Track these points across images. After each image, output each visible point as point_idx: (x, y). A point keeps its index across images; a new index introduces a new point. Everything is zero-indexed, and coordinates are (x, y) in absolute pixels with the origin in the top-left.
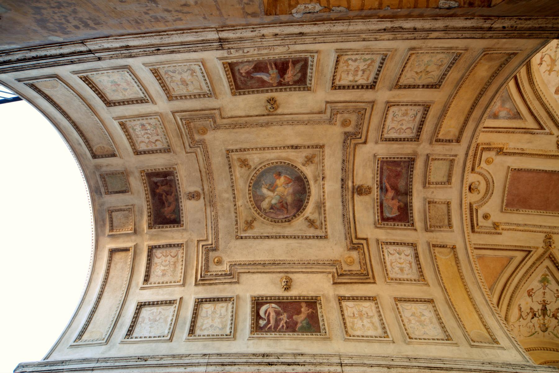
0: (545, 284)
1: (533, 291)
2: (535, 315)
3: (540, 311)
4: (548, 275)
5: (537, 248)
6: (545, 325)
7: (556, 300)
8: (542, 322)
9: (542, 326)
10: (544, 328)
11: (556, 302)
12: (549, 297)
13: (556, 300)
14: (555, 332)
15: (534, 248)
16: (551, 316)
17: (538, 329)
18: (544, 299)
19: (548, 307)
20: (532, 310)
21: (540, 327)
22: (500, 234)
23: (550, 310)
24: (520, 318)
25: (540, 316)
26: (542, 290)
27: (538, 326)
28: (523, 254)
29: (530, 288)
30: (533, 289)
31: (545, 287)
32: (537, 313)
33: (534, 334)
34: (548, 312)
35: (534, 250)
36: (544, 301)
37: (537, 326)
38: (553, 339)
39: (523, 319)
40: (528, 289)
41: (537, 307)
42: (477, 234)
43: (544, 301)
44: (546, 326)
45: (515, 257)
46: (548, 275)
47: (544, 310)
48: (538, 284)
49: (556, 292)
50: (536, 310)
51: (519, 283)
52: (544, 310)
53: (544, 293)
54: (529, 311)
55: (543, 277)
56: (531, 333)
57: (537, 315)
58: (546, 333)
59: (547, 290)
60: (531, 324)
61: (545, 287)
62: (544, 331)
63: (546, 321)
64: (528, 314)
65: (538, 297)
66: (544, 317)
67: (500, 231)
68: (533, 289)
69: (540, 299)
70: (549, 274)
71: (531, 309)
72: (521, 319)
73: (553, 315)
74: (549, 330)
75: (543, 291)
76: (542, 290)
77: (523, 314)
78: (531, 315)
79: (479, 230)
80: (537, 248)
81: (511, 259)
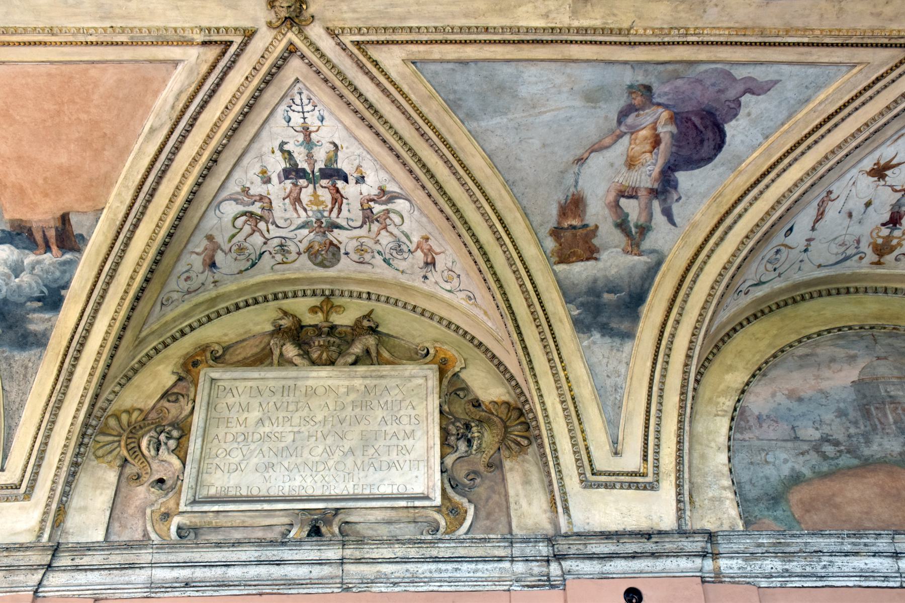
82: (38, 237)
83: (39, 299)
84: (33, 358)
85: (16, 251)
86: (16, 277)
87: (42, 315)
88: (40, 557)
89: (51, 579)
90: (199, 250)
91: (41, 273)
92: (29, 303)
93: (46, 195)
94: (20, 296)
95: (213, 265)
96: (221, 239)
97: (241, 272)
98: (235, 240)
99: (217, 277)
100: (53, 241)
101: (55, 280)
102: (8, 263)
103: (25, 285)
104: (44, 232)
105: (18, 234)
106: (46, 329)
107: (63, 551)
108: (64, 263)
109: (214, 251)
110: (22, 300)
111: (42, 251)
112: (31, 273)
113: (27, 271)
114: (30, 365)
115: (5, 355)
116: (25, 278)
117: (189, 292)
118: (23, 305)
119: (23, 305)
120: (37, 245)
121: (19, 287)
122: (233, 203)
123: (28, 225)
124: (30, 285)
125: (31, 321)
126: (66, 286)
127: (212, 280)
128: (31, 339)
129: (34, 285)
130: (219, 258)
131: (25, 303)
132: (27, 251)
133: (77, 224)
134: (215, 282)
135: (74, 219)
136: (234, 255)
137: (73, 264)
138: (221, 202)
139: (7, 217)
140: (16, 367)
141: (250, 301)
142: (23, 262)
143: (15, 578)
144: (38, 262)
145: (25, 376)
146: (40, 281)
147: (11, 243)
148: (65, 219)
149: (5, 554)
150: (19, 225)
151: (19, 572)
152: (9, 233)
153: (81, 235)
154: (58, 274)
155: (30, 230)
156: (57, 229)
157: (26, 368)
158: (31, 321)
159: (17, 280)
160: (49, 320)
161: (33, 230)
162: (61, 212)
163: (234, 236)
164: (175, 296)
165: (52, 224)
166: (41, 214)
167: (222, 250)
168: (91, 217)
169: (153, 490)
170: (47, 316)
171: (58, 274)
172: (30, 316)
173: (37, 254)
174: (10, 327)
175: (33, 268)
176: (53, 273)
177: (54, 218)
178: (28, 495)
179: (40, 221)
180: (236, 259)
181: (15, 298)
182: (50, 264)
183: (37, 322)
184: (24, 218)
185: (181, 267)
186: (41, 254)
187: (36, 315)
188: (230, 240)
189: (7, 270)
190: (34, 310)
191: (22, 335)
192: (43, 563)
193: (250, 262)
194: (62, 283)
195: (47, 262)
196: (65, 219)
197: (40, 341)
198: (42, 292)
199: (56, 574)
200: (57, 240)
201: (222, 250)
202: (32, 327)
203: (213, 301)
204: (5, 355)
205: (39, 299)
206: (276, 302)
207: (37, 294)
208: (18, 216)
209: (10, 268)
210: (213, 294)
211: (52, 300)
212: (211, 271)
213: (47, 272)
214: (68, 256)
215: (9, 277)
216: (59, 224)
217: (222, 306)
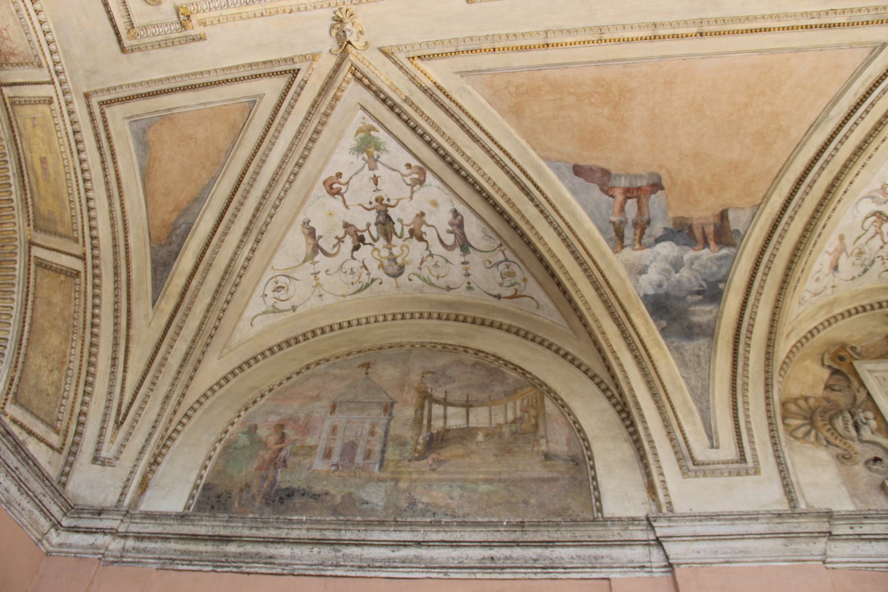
0: (371, 156)
1: (343, 180)
2: (362, 239)
3: (374, 230)
4: (374, 129)
5: (314, 57)
6: (395, 260)
7: (412, 192)
8: (385, 253)
9: (386, 263)
10: (394, 269)
11: (411, 198)
12: (392, 187)
13: (412, 192)
14: (425, 273)
15: (304, 57)
16: (407, 234)
17: (376, 272)
18: (377, 194)
19: (391, 212)
20: (352, 230)
21: (381, 266)
22: (201, 38)
23: (400, 221)
24: (315, 253)
25: (375, 240)
26: (368, 174)
27: (377, 264)
28: (280, 83)
29: (329, 172)
30: (339, 175)
31: (373, 163)
32: (366, 235)
33: (367, 285)
34: (398, 227)
35: (303, 66)
36: (379, 200)
37: (373, 266)
38: (422, 292)
39: (326, 254)
40: (324, 176)
41: (364, 220)
42: (137, 54)
43: (379, 200)
44: (399, 260)
45: (261, 96)
46: (374, 129)
47: (386, 224)
48: (353, 158)
49: (405, 171)
50: (361, 226)
51: (280, 167)
52: (386, 224)
53: (376, 180)
54: (341, 232)
55: (362, 135)
56: (358, 286)
57: (368, 240)
58: (403, 278)
59: (381, 171)
60: (356, 265)
61: (373, 163)
62: (395, 276)
63: (396, 251)
64: (340, 240)
65: (360, 191)
66: (388, 239)
67: (197, 30)
68: (339, 175)
69: (368, 196)
70: (375, 125)
71: (346, 226)
72: (320, 257)
73: (412, 232)
74: (408, 270)
75: (371, 174)
76: (368, 174)
77: (321, 243)
78: (349, 242)
79: (134, 42)
80: (314, 57)
81: (252, 103)
82: (698, 233)
83: (698, 293)
84: (703, 348)
85: (677, 248)
86: (677, 272)
87: (703, 308)
88: (816, 525)
89: (833, 549)
90: (831, 250)
91: (699, 268)
92: (689, 297)
93: (710, 192)
94: (680, 290)
95: (836, 268)
96: (848, 242)
97: (854, 278)
98: (858, 243)
99: (836, 284)
100: (711, 237)
101: (713, 275)
102: (669, 259)
103: (684, 280)
104: (703, 228)
105: (679, 231)
106: (709, 321)
107: (838, 519)
108: (725, 257)
109: (841, 252)
110: (683, 294)
111: (701, 247)
112: (690, 268)
113: (686, 266)
114: (701, 353)
115: (675, 345)
116: (685, 273)
117: (816, 295)
118: (684, 298)
119: (684, 298)
120: (696, 241)
121: (679, 281)
122: (870, 200)
123: (689, 222)
124: (689, 280)
125: (694, 314)
126: (725, 279)
127: (831, 284)
128: (696, 330)
129: (693, 279)
130: (843, 262)
131: (686, 296)
132: (686, 248)
133: (737, 220)
134: (833, 287)
135: (731, 215)
136: (853, 259)
137: (732, 260)
138: (860, 200)
139: (671, 215)
140: (688, 356)
141: (860, 309)
142: (682, 258)
143: (796, 546)
144: (697, 258)
145: (699, 364)
146: (699, 276)
147: (672, 240)
148: (723, 215)
149: (778, 521)
150: (681, 223)
151: (798, 540)
152: (671, 230)
153: (737, 231)
154: (715, 269)
155: (690, 227)
156: (715, 226)
157: (698, 356)
158: (694, 314)
159: (677, 275)
160: (711, 312)
161: (694, 227)
162: (721, 209)
163: (859, 238)
164: (807, 296)
165: (712, 220)
166: (702, 213)
167: (846, 252)
168: (748, 214)
169: (875, 467)
170: (708, 308)
171: (715, 269)
172: (692, 309)
173: (695, 250)
174: (675, 320)
175: (692, 263)
176: (711, 268)
177: (714, 215)
178: (757, 472)
179: (701, 218)
180: (853, 264)
181: (676, 293)
182: (708, 260)
183: (701, 314)
184: (686, 216)
185: (816, 268)
186: (699, 250)
187: (698, 308)
188: (855, 243)
189: (667, 266)
190: (696, 303)
191: (687, 326)
192: (825, 530)
193: (862, 269)
194: (720, 276)
195: (705, 257)
196: (723, 215)
197: (709, 332)
198: (701, 286)
199: (838, 544)
200: (715, 236)
201: (846, 252)
202: (695, 319)
203: (831, 304)
204: (675, 345)
205: (698, 293)
206: (881, 311)
207: (696, 288)
208: (680, 214)
209: (671, 264)
210: (831, 298)
211: (713, 293)
212: (833, 274)
213: (705, 267)
214: (724, 251)
215: (670, 273)
216: (717, 221)
217: (837, 311)
